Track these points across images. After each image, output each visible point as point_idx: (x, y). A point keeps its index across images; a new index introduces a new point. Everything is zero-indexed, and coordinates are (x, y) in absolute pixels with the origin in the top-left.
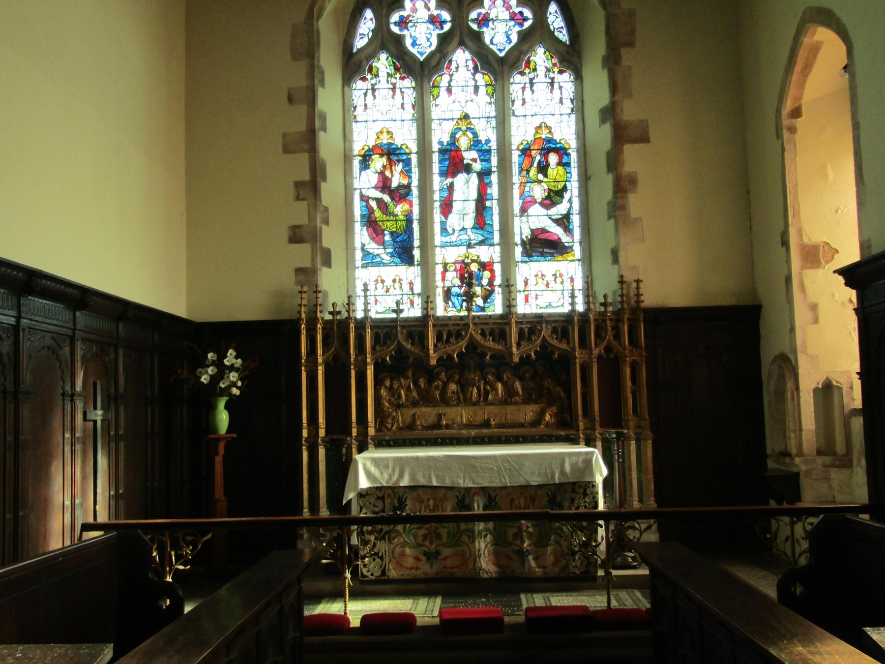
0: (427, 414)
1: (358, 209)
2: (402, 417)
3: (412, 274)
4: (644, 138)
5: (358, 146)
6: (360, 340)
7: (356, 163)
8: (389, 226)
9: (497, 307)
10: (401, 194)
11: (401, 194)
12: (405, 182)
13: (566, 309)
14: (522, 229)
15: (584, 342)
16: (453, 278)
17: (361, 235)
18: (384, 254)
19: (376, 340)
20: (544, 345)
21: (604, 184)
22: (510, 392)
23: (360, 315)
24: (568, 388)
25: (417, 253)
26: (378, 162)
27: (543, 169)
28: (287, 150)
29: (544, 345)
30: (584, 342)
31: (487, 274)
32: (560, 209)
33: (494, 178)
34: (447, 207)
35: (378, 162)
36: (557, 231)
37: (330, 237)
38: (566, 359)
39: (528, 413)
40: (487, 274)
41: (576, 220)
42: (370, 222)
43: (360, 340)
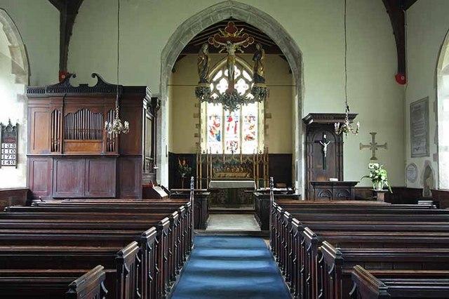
0: (223, 174)
1: (209, 129)
2: (218, 174)
3: (220, 143)
4: (271, 118)
5: (209, 115)
6: (209, 159)
7: (208, 118)
8: (215, 132)
9: (238, 152)
10: (218, 126)
11: (218, 126)
12: (219, 123)
13: (252, 153)
14: (244, 135)
15: (256, 160)
16: (229, 145)
17: (209, 133)
18: (214, 139)
19: (213, 159)
20: (248, 160)
21: (262, 126)
22: (240, 170)
23: (209, 153)
24: (253, 170)
25: (221, 139)
26: (213, 118)
27: (249, 121)
28: (194, 117)
29: (248, 160)
30: (256, 160)
31: (236, 144)
32: (252, 131)
33: (239, 123)
34: (228, 129)
35: (213, 118)
36: (252, 135)
37: (203, 136)
38: (252, 164)
39: (244, 174)
40: (236, 144)
41: (256, 134)
42: (211, 132)
43: (209, 159)
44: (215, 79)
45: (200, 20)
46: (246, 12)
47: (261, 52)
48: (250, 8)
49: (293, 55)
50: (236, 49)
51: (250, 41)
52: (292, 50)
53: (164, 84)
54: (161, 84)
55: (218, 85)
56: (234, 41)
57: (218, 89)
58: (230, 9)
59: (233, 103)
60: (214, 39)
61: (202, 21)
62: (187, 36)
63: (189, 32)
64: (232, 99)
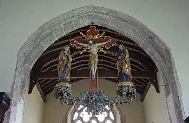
44: (79, 109)
45: (62, 24)
46: (108, 17)
47: (124, 51)
48: (110, 12)
49: (159, 52)
50: (99, 50)
51: (113, 42)
52: (157, 49)
53: (19, 83)
54: (14, 82)
55: (81, 113)
56: (96, 42)
57: (81, 116)
58: (92, 15)
59: (96, 103)
60: (75, 41)
61: (64, 25)
62: (48, 38)
63: (50, 34)
64: (95, 100)
